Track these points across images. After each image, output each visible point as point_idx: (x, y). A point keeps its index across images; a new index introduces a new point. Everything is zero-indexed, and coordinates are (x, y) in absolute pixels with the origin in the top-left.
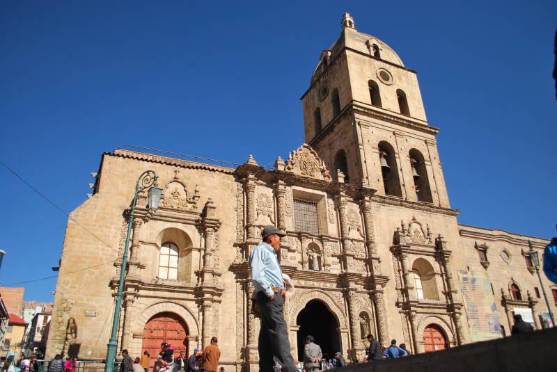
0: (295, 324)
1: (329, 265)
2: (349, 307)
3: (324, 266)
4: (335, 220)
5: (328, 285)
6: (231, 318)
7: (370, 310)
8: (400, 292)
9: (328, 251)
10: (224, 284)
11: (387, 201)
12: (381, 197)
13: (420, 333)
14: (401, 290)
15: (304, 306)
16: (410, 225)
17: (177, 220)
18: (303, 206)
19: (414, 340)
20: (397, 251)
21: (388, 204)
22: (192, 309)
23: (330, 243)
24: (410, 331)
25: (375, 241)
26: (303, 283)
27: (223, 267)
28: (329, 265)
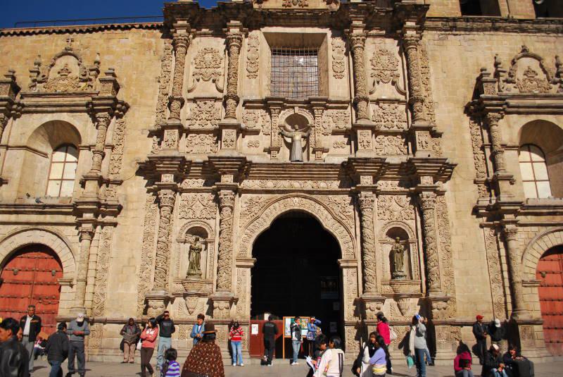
0: (249, 255)
1: (324, 151)
2: (361, 221)
3: (314, 152)
4: (346, 73)
5: (323, 185)
6: (132, 250)
7: (411, 224)
8: (483, 187)
9: (325, 125)
10: (126, 195)
11: (463, 24)
12: (447, 20)
13: (530, 264)
14: (487, 183)
15: (267, 224)
16: (513, 63)
17: (60, 108)
18: (283, 58)
19: (511, 279)
20: (479, 111)
21: (465, 30)
22: (70, 238)
23: (330, 111)
24: (504, 260)
25: (434, 97)
26: (270, 184)
27: (127, 169)
28: (324, 151)
